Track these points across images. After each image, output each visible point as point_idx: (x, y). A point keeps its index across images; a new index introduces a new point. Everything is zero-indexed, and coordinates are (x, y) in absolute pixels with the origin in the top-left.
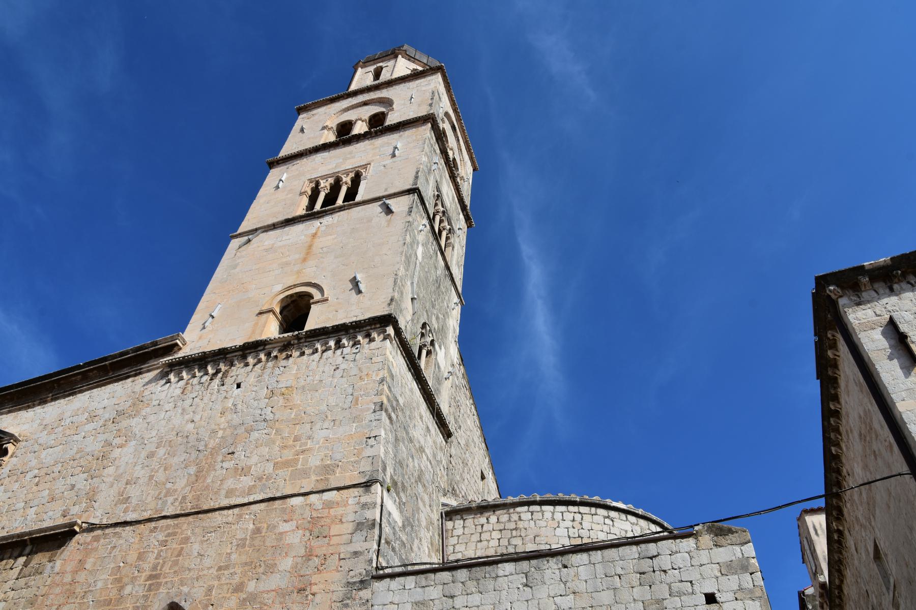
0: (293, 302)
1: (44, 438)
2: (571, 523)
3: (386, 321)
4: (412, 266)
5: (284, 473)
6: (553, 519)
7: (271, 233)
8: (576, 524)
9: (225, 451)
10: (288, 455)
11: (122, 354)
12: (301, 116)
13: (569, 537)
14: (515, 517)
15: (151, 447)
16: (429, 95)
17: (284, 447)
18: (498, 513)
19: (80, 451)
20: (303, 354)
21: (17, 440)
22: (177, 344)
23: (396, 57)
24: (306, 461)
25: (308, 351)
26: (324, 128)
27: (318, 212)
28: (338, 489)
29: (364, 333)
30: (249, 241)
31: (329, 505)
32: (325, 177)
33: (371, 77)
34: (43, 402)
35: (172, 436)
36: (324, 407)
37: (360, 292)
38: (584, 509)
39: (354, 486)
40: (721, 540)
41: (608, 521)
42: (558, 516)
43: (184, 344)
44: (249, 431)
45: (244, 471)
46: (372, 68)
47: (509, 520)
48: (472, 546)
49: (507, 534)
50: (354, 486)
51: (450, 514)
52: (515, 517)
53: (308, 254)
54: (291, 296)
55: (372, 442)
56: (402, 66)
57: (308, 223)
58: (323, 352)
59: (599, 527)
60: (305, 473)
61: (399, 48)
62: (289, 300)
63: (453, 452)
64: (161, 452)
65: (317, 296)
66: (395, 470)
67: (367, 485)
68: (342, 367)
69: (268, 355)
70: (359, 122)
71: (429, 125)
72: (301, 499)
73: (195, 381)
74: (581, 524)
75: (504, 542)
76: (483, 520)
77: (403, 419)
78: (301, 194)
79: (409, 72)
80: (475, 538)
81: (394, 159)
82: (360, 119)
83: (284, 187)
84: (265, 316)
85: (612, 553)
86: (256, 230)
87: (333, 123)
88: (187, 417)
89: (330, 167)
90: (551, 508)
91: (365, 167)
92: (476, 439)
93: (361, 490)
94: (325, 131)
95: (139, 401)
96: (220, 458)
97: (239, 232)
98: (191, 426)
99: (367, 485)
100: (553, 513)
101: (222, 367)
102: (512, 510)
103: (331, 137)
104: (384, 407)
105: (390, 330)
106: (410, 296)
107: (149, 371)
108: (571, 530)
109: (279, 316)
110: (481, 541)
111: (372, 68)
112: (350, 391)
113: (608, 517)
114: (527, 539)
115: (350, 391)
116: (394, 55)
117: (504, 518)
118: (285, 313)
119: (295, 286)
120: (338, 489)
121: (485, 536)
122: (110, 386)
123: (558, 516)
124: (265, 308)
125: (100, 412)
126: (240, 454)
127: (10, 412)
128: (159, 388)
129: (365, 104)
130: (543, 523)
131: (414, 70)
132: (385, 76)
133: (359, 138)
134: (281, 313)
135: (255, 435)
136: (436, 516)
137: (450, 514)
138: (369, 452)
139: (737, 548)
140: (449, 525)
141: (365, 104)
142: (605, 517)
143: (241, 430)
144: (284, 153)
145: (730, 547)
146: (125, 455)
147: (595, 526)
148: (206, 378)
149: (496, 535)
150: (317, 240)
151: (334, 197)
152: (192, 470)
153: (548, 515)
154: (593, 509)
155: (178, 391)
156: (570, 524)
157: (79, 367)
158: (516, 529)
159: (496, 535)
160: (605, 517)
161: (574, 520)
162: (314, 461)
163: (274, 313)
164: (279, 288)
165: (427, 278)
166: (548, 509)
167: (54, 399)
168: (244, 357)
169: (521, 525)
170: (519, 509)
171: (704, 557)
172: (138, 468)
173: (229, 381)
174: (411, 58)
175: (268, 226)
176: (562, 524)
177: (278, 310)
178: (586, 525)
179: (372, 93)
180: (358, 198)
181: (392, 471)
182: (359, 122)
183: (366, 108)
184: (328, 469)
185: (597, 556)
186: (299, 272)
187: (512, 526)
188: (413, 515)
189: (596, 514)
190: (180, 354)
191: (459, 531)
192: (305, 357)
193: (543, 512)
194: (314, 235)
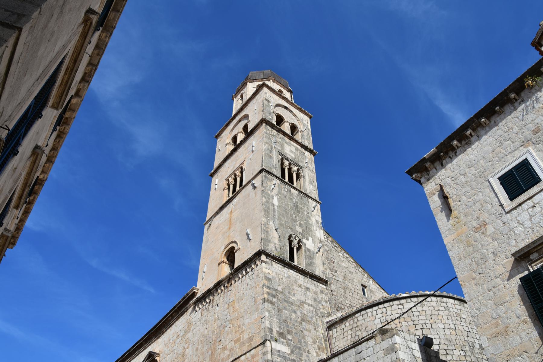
0: (231, 252)
1: (167, 351)
2: (381, 315)
3: (259, 254)
4: (271, 213)
5: (238, 345)
6: (372, 315)
7: (217, 217)
8: (384, 315)
9: (218, 340)
10: (238, 336)
11: (179, 303)
12: (218, 140)
13: (381, 323)
14: (356, 320)
15: (196, 346)
16: (262, 104)
17: (236, 332)
18: (348, 320)
19: (177, 354)
20: (235, 281)
21: (159, 354)
22: (195, 292)
23: (247, 84)
24: (243, 337)
25: (237, 279)
26: (226, 145)
27: (238, 191)
28: (255, 348)
29: (254, 263)
30: (210, 225)
31: (253, 357)
32: (230, 176)
33: (240, 101)
34: (163, 333)
35: (201, 338)
36: (246, 307)
37: (250, 240)
38: (386, 305)
39: (260, 345)
40: (384, 337)
41: (400, 307)
42: (374, 313)
43: (198, 290)
44: (224, 328)
45: (225, 348)
46: (239, 97)
47: (354, 323)
48: (341, 341)
49: (354, 330)
50: (260, 345)
51: (331, 326)
52: (356, 320)
53: (230, 224)
54: (228, 250)
55: (263, 320)
56: (251, 88)
57: (228, 206)
58: (242, 277)
59: (396, 312)
60: (243, 344)
61: (247, 78)
62: (229, 253)
63: (333, 287)
64: (200, 346)
65: (236, 248)
66: (280, 327)
67: (263, 343)
68: (249, 284)
69: (224, 286)
70: (239, 134)
71: (264, 124)
72: (244, 356)
73: (204, 308)
74: (386, 313)
75: (353, 335)
76: (343, 326)
77: (283, 297)
78: (224, 189)
79: (255, 89)
80: (342, 337)
81: (254, 152)
82: (239, 133)
83: (218, 187)
84: (221, 265)
85: (346, 354)
86: (211, 217)
87: (229, 140)
88: (204, 327)
89: (232, 168)
90: (370, 310)
91: (243, 163)
92: (352, 270)
93: (262, 346)
94: (227, 146)
95: (189, 324)
96: (217, 344)
97: (207, 220)
98: (206, 331)
99: (263, 343)
100: (372, 312)
101: (211, 298)
102: (354, 317)
103: (232, 147)
104: (266, 299)
105: (263, 257)
106: (274, 229)
107: (190, 307)
108: (382, 319)
109: (227, 262)
110: (344, 337)
111: (239, 97)
112: (253, 295)
113: (400, 304)
114: (363, 330)
115: (253, 295)
116: (244, 85)
117: (351, 322)
118: (229, 259)
119: (228, 245)
120: (255, 348)
121: (346, 334)
122: (180, 319)
123: (374, 313)
124: (220, 261)
125: (179, 333)
126: (223, 340)
127: (155, 341)
128: (194, 315)
129: (240, 121)
130: (368, 320)
131: (257, 86)
132: (246, 97)
133: (243, 142)
134: (228, 260)
135: (226, 329)
136: (321, 331)
137: (331, 326)
138: (263, 326)
139: (390, 340)
140: (331, 332)
141: (240, 121)
142: (398, 305)
143: (222, 329)
144: (216, 165)
145: (387, 340)
146: (189, 352)
147: (394, 312)
148: (207, 305)
149: (350, 332)
150: (232, 215)
151: (236, 186)
152: (210, 352)
153: (370, 314)
154: (391, 303)
155: (200, 315)
156: (380, 315)
157: (168, 314)
158: (357, 326)
159: (350, 332)
160: (398, 305)
161: (382, 313)
162: (246, 336)
163: (224, 262)
164: (223, 248)
165: (285, 211)
166: (369, 310)
167: (166, 330)
168: (217, 290)
169: (359, 323)
170: (357, 315)
171: (378, 348)
172: (194, 357)
173: (214, 304)
174: (254, 81)
175: (215, 214)
176: (377, 317)
177: (225, 260)
178: (389, 313)
179: (241, 114)
180: (244, 184)
181: (278, 329)
182: (239, 134)
183: (240, 123)
184: (250, 339)
185: (341, 356)
186: (229, 236)
187: (355, 325)
188: (300, 342)
189: (393, 305)
190: (198, 296)
191: (335, 335)
192: (237, 283)
193: (367, 313)
194: (231, 212)
